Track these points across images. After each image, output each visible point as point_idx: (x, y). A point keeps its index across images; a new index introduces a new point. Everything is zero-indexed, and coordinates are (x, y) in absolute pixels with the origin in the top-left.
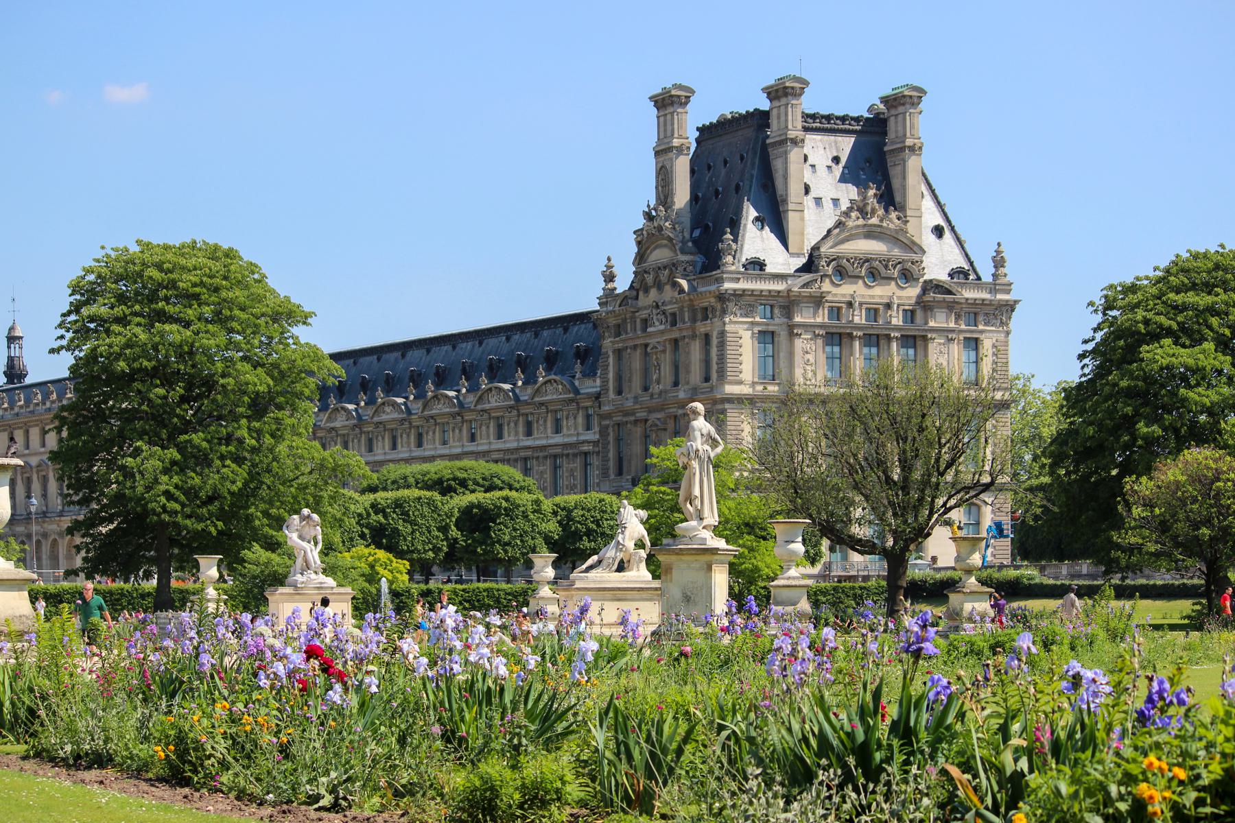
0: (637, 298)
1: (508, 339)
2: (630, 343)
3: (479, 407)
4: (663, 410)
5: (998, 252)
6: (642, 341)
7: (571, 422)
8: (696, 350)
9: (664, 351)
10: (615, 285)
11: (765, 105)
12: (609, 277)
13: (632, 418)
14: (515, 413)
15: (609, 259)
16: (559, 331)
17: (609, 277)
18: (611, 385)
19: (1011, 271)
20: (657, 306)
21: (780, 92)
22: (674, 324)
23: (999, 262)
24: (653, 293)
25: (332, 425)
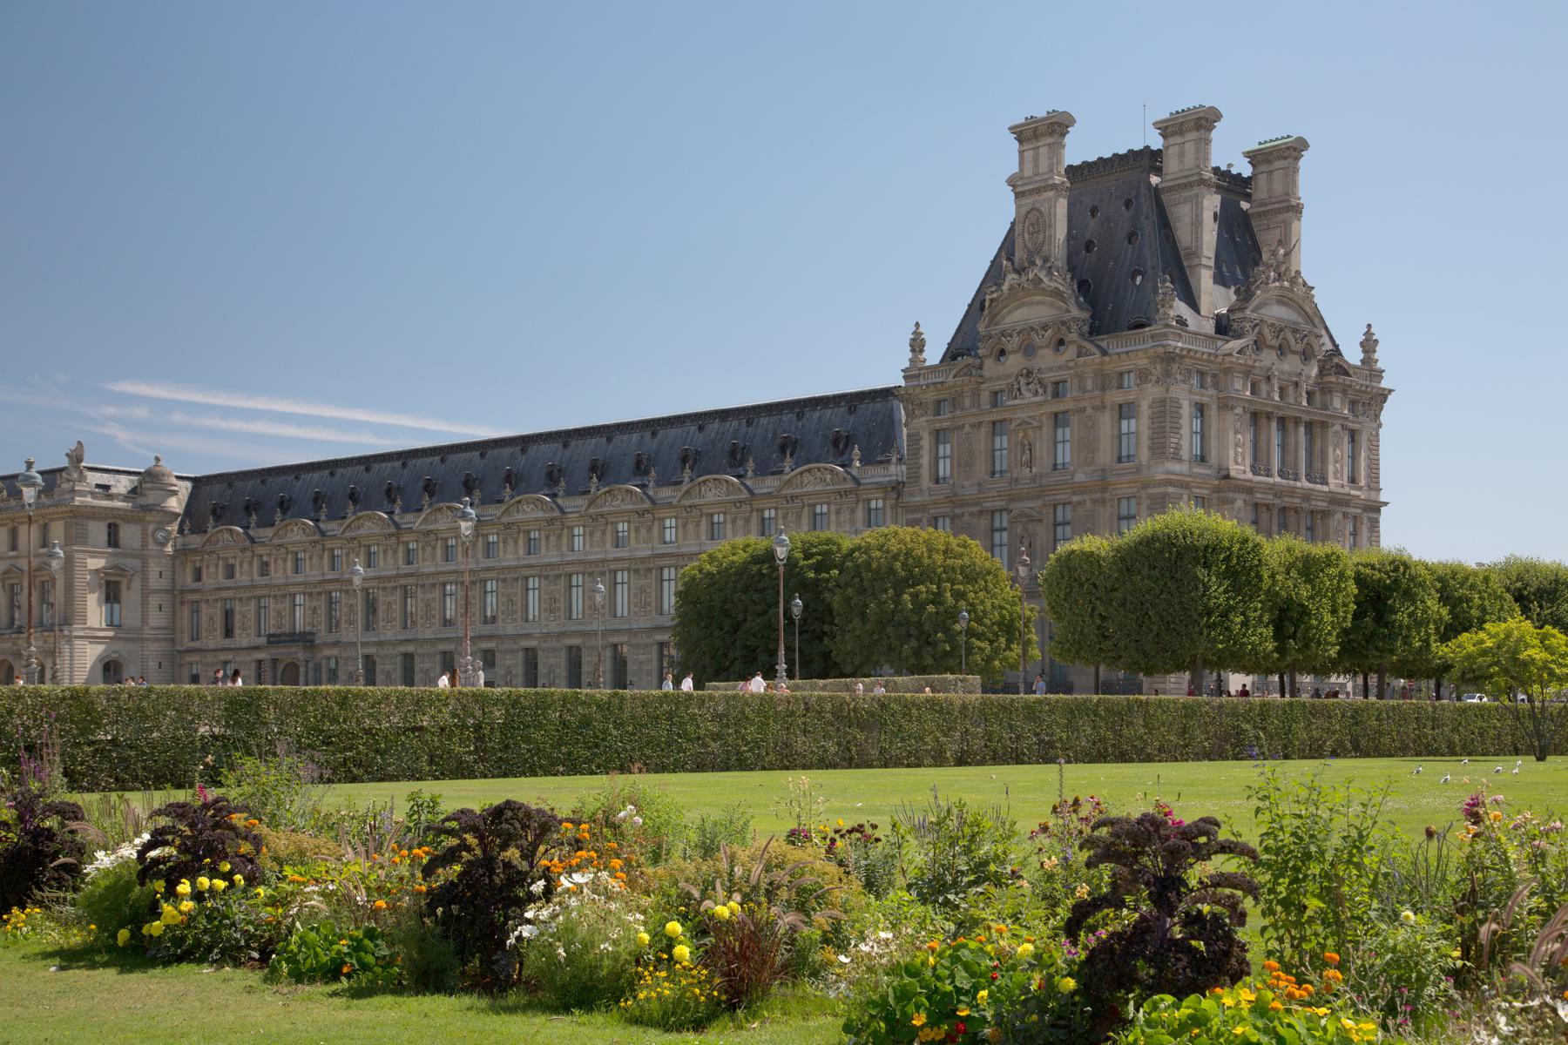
0: (981, 368)
1: (701, 428)
2: (973, 420)
3: (686, 503)
4: (1039, 497)
5: (1368, 334)
6: (995, 417)
7: (845, 516)
8: (1106, 421)
9: (1040, 428)
10: (925, 355)
12: (917, 345)
13: (977, 509)
14: (746, 508)
15: (917, 325)
16: (843, 410)
17: (917, 345)
18: (925, 471)
19: (1382, 357)
20: (1029, 374)
22: (1056, 395)
23: (1369, 344)
24: (1014, 362)
25: (431, 527)
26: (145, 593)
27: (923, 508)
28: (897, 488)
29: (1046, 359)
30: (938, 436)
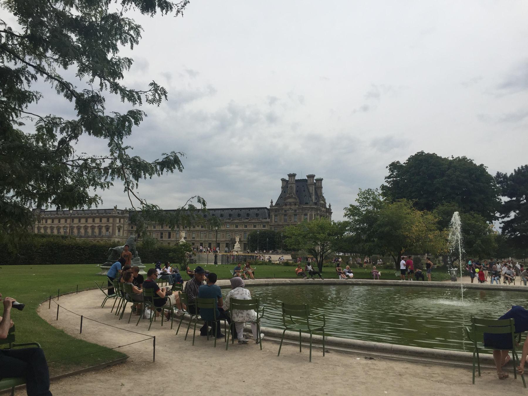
11: (307, 178)
12: (272, 202)
17: (272, 202)
21: (311, 177)
24: (288, 207)
26: (124, 230)
27: (273, 225)
28: (268, 222)
29: (293, 207)
30: (276, 216)
